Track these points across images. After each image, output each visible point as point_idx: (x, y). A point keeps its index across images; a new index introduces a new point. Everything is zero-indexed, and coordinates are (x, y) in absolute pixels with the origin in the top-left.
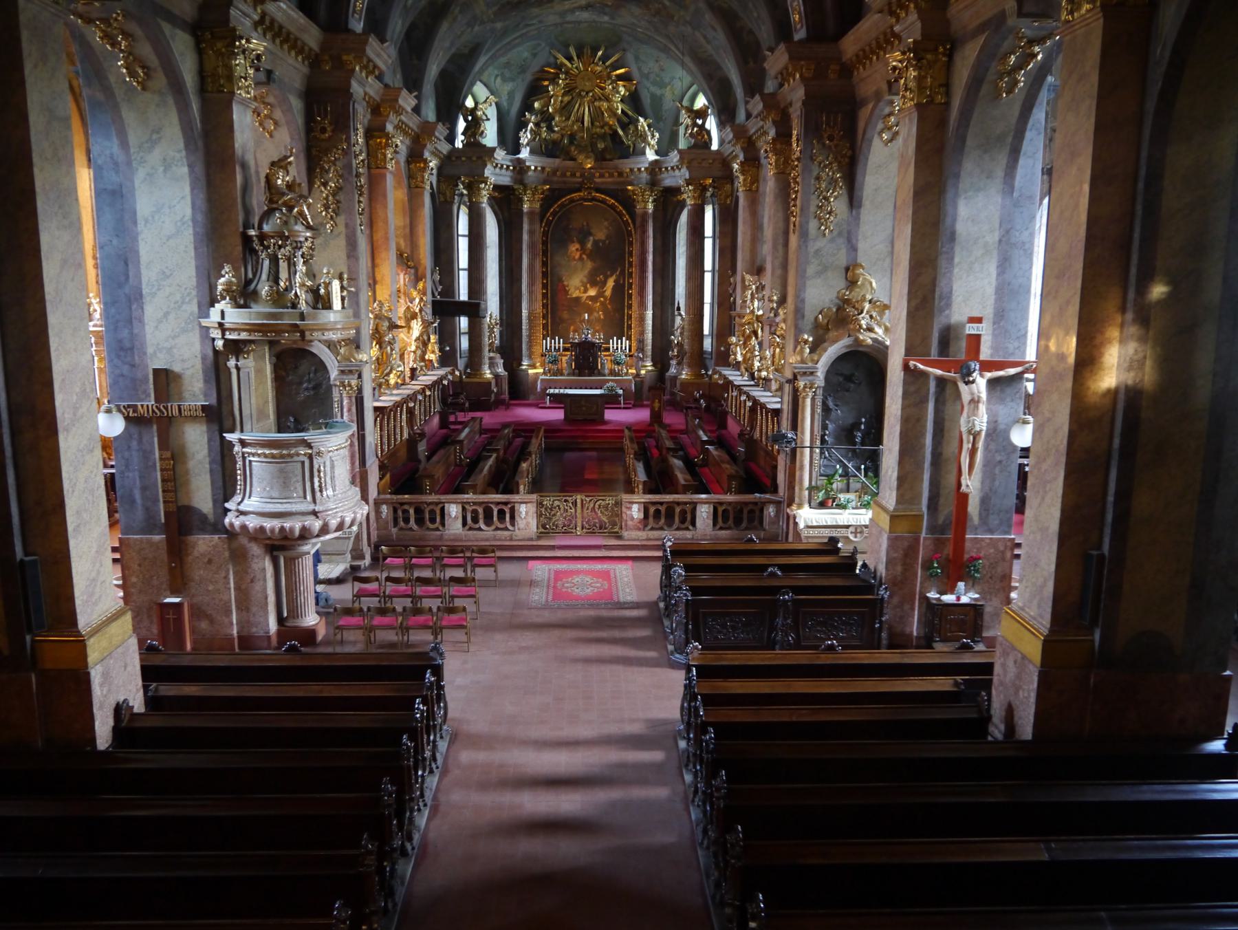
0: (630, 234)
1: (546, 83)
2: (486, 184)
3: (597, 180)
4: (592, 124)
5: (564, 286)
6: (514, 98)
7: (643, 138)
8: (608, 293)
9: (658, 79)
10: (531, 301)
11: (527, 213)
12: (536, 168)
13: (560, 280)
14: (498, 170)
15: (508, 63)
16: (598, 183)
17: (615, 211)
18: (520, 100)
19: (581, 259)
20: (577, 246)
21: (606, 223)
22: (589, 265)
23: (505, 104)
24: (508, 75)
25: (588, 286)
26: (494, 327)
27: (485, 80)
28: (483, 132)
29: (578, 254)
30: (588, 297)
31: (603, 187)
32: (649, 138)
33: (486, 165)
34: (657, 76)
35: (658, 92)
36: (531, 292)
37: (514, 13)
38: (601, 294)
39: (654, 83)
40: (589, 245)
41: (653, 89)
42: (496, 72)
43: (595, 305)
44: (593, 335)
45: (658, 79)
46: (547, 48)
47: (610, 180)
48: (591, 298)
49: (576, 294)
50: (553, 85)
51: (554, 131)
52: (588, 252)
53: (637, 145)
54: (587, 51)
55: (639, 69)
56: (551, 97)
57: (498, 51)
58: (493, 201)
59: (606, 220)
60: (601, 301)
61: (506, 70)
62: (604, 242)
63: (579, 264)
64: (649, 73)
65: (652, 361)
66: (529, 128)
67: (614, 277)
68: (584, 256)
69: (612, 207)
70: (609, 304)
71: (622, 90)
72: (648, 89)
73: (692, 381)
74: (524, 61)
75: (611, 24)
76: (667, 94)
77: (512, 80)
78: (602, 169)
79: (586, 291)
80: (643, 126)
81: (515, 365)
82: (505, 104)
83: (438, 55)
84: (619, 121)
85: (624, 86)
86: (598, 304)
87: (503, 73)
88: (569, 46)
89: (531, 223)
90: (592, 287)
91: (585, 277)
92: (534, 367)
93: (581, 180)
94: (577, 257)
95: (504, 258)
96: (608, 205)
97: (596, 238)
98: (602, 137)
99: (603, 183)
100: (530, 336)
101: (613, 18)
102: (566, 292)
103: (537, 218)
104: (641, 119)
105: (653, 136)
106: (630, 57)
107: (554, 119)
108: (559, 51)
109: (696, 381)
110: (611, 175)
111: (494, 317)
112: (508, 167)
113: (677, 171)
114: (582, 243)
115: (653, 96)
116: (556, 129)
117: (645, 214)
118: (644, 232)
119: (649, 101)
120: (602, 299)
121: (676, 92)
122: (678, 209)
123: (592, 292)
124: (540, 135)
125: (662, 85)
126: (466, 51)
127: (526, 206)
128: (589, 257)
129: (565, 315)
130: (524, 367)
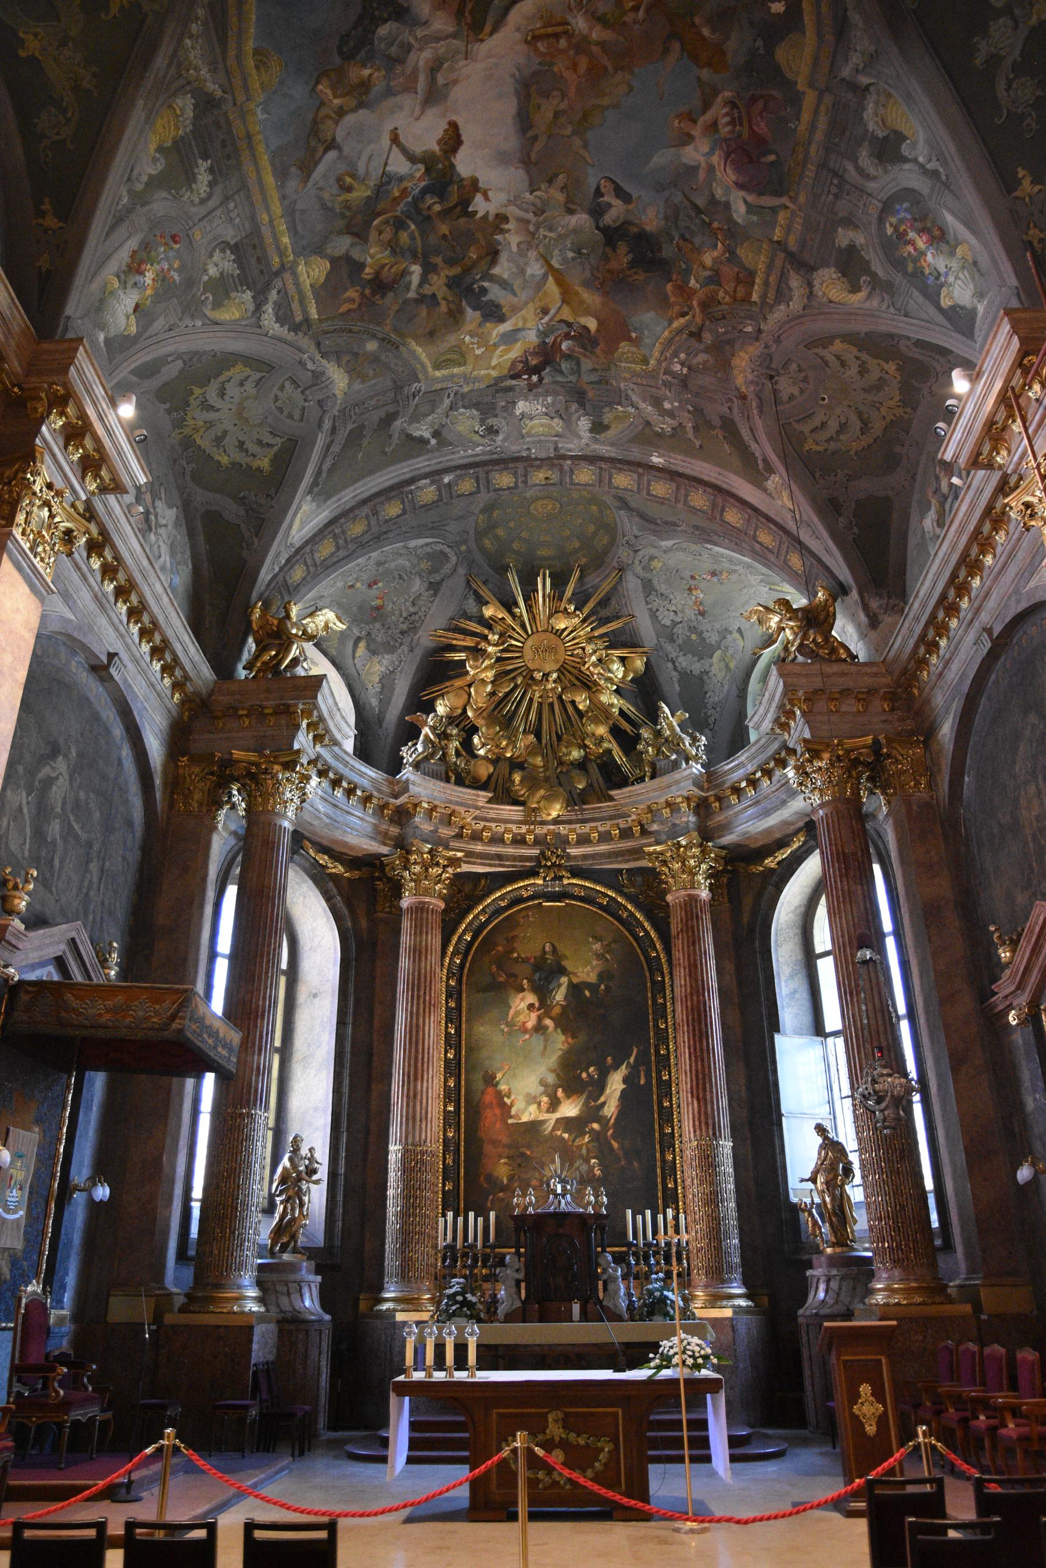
0: (654, 965)
1: (462, 656)
2: (293, 770)
3: (573, 851)
4: (559, 738)
5: (500, 1095)
6: (392, 691)
7: (674, 744)
8: (611, 1109)
9: (694, 637)
10: (411, 1119)
11: (410, 909)
12: (434, 809)
13: (490, 1080)
14: (339, 793)
15: (379, 608)
16: (575, 857)
17: (619, 919)
18: (405, 691)
19: (539, 1028)
20: (531, 998)
21: (597, 946)
22: (560, 1042)
23: (374, 702)
24: (380, 637)
25: (560, 1093)
26: (299, 1179)
27: (333, 652)
28: (295, 662)
29: (534, 1016)
30: (558, 1120)
31: (586, 864)
32: (687, 741)
33: (298, 727)
34: (693, 629)
35: (697, 668)
36: (412, 1097)
37: (372, 346)
38: (592, 1113)
39: (687, 648)
40: (559, 996)
41: (684, 662)
42: (356, 632)
43: (578, 1142)
44: (579, 1196)
45: (694, 637)
46: (462, 571)
47: (603, 848)
48: (567, 1123)
49: (529, 1114)
50: (476, 659)
51: (476, 756)
52: (557, 1011)
53: (662, 764)
54: (544, 586)
55: (653, 614)
56: (470, 686)
57: (346, 514)
58: (331, 885)
59: (597, 938)
60: (593, 1129)
61: (378, 625)
62: (593, 987)
63: (537, 1042)
64: (675, 624)
65: (745, 1283)
66: (422, 738)
67: (623, 1070)
68: (548, 1022)
69: (611, 909)
70: (614, 1136)
71: (618, 671)
72: (673, 662)
73: (914, 1310)
74: (414, 604)
75: (591, 459)
76: (714, 670)
77: (391, 649)
78: (584, 821)
79: (554, 1105)
80: (671, 727)
81: (363, 1306)
82: (374, 702)
83: (135, 267)
84: (616, 732)
85: (623, 660)
86: (587, 1139)
87: (369, 634)
88: (506, 568)
89: (419, 929)
90: (570, 1093)
91: (552, 1071)
92: (409, 1302)
93: (535, 852)
94: (532, 1020)
95: (350, 1019)
96: (601, 907)
97: (575, 980)
98: (582, 765)
99: (585, 857)
100: (405, 1215)
101: (598, 427)
102: (506, 1109)
103: (435, 922)
104: (666, 709)
105: (694, 740)
106: (632, 583)
107: (474, 730)
108: (485, 583)
109: (931, 1310)
110: (606, 837)
111: (304, 1151)
112: (367, 799)
113: (765, 783)
114: (543, 992)
115: (685, 677)
116: (482, 752)
117: (693, 899)
118: (694, 941)
119: (677, 688)
120: (596, 1126)
121: (732, 665)
122: (770, 889)
123: (570, 1109)
124: (444, 749)
125: (704, 650)
126: (265, 463)
127: (406, 902)
128: (558, 1022)
129: (502, 1170)
130: (385, 1306)
